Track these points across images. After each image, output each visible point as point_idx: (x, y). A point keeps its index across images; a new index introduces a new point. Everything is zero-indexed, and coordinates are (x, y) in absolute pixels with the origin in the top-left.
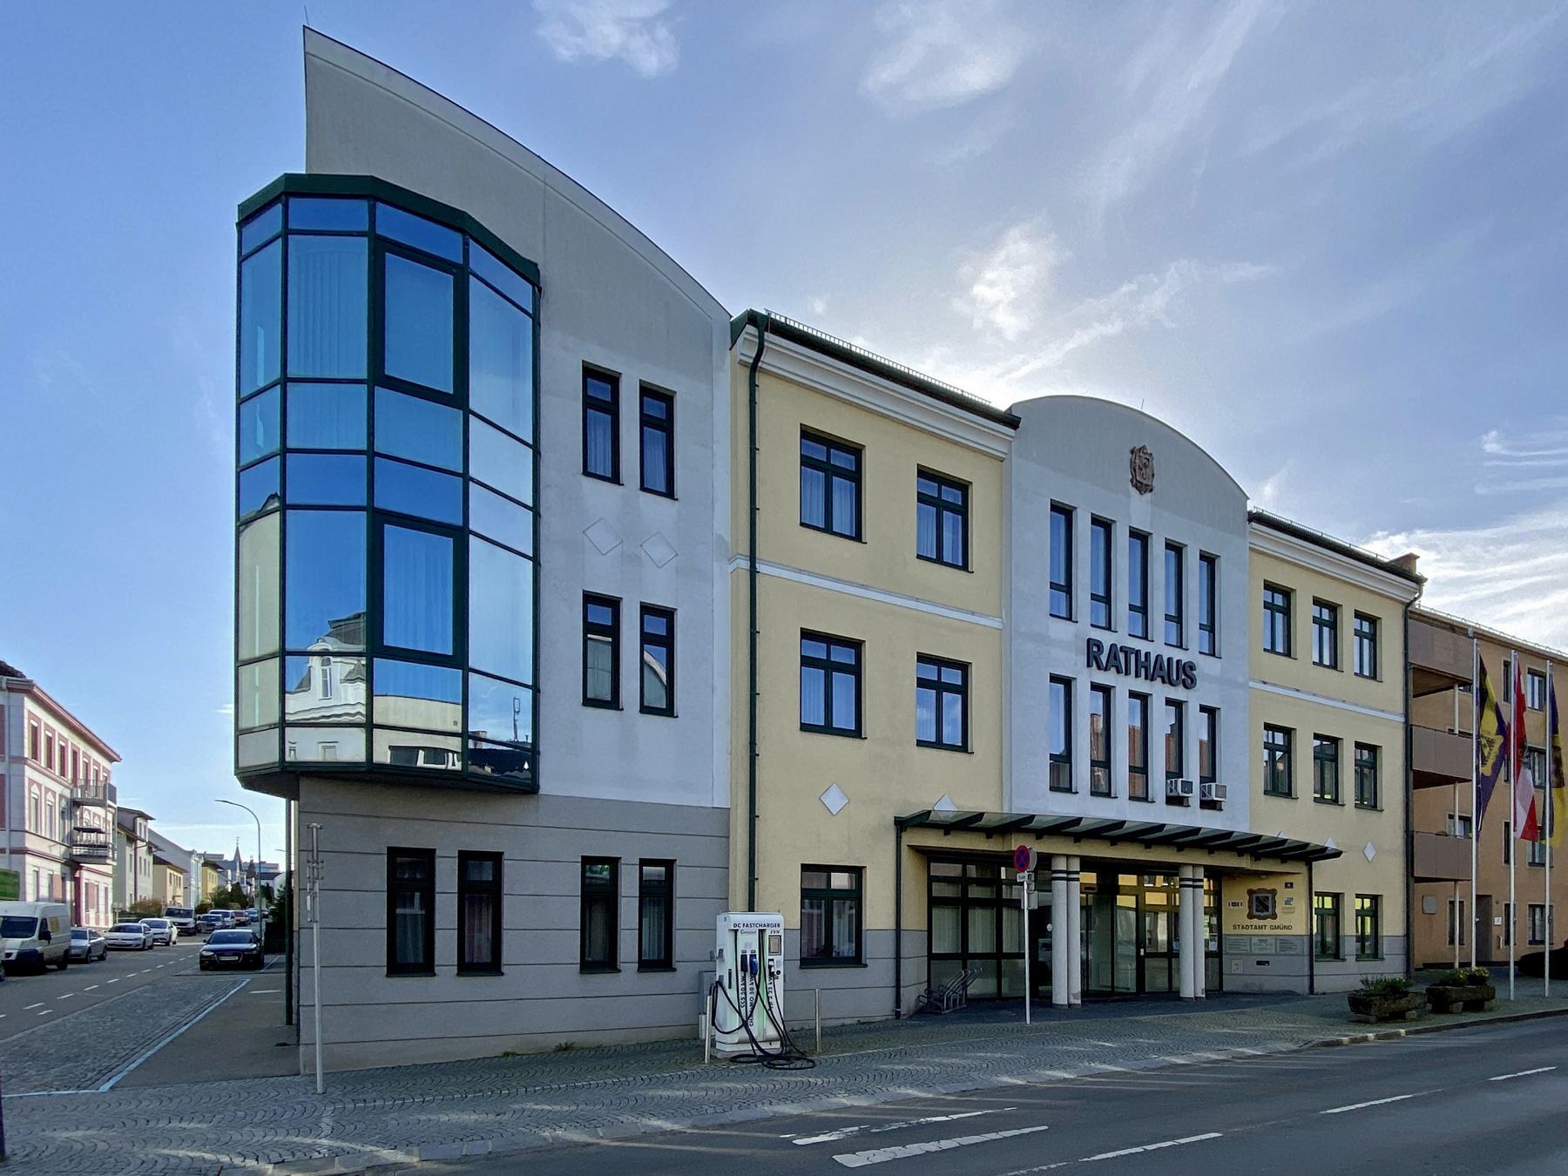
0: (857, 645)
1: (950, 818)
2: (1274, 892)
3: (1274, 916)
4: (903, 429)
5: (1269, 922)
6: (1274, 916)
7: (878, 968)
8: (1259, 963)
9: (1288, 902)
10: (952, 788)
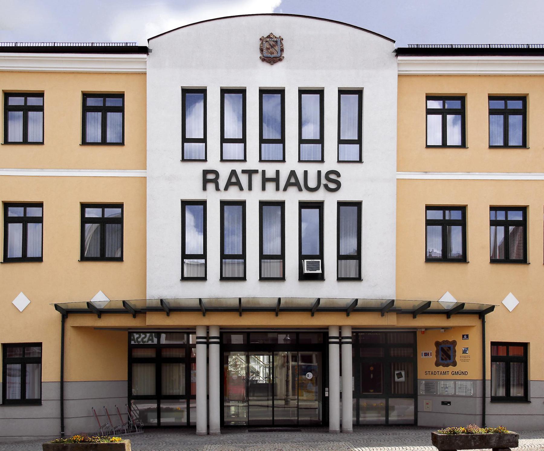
0: (463, 209)
1: (450, 307)
2: (454, 343)
3: (455, 364)
4: (72, 76)
5: (451, 368)
6: (455, 364)
7: (50, 407)
8: (443, 403)
9: (465, 352)
10: (102, 286)
